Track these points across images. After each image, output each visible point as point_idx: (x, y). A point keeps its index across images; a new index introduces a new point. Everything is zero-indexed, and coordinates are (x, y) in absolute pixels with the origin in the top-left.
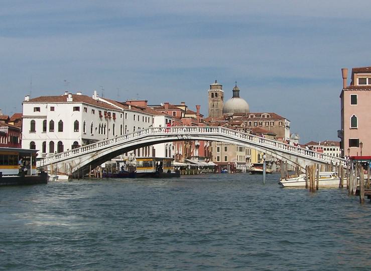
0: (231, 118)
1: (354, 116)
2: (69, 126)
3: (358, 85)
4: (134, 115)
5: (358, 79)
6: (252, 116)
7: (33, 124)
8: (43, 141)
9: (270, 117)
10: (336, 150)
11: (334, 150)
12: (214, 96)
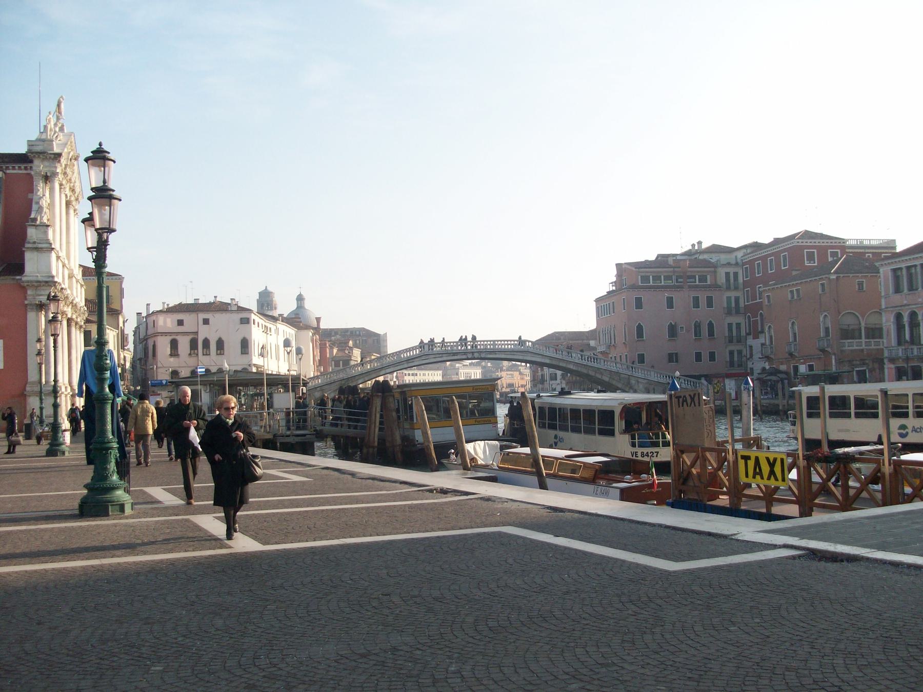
1: (639, 324)
2: (233, 346)
7: (174, 344)
8: (192, 368)
10: (418, 375)
11: (416, 375)
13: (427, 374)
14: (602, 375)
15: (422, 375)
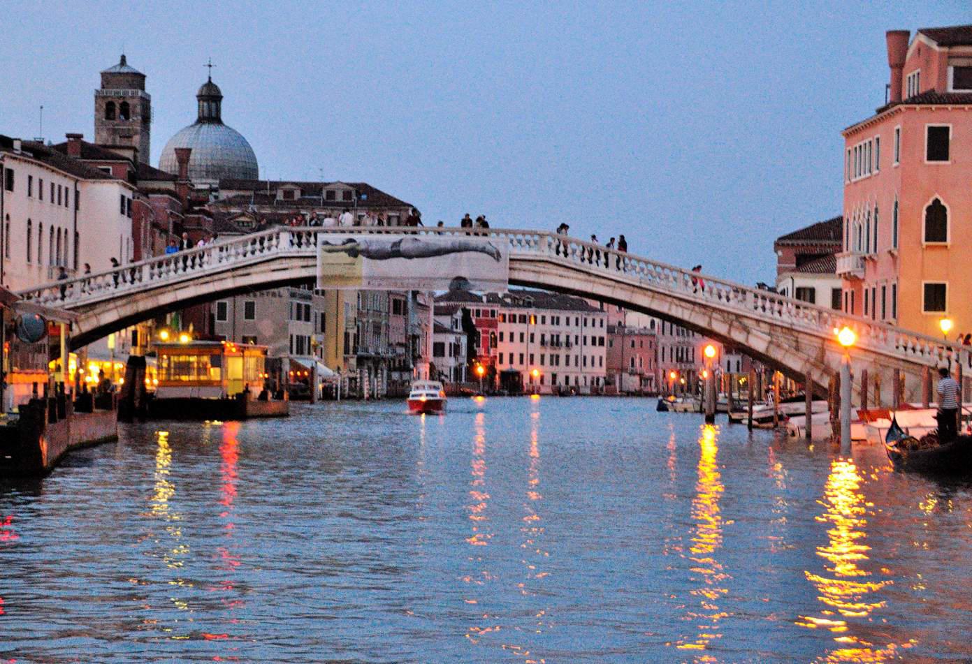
0: (212, 199)
1: (937, 202)
3: (951, 90)
4: (30, 178)
5: (951, 71)
6: (289, 194)
9: (354, 197)
12: (118, 111)
13: (563, 321)
14: (748, 333)
15: (548, 320)
